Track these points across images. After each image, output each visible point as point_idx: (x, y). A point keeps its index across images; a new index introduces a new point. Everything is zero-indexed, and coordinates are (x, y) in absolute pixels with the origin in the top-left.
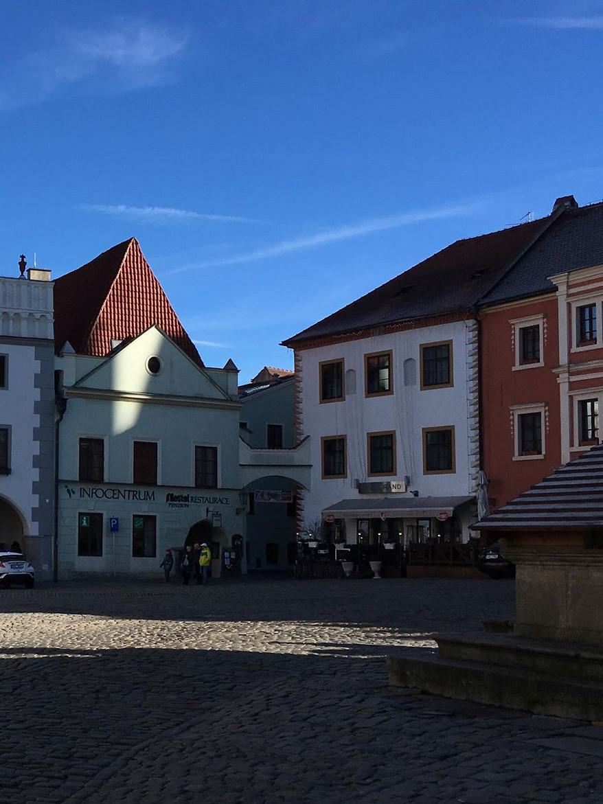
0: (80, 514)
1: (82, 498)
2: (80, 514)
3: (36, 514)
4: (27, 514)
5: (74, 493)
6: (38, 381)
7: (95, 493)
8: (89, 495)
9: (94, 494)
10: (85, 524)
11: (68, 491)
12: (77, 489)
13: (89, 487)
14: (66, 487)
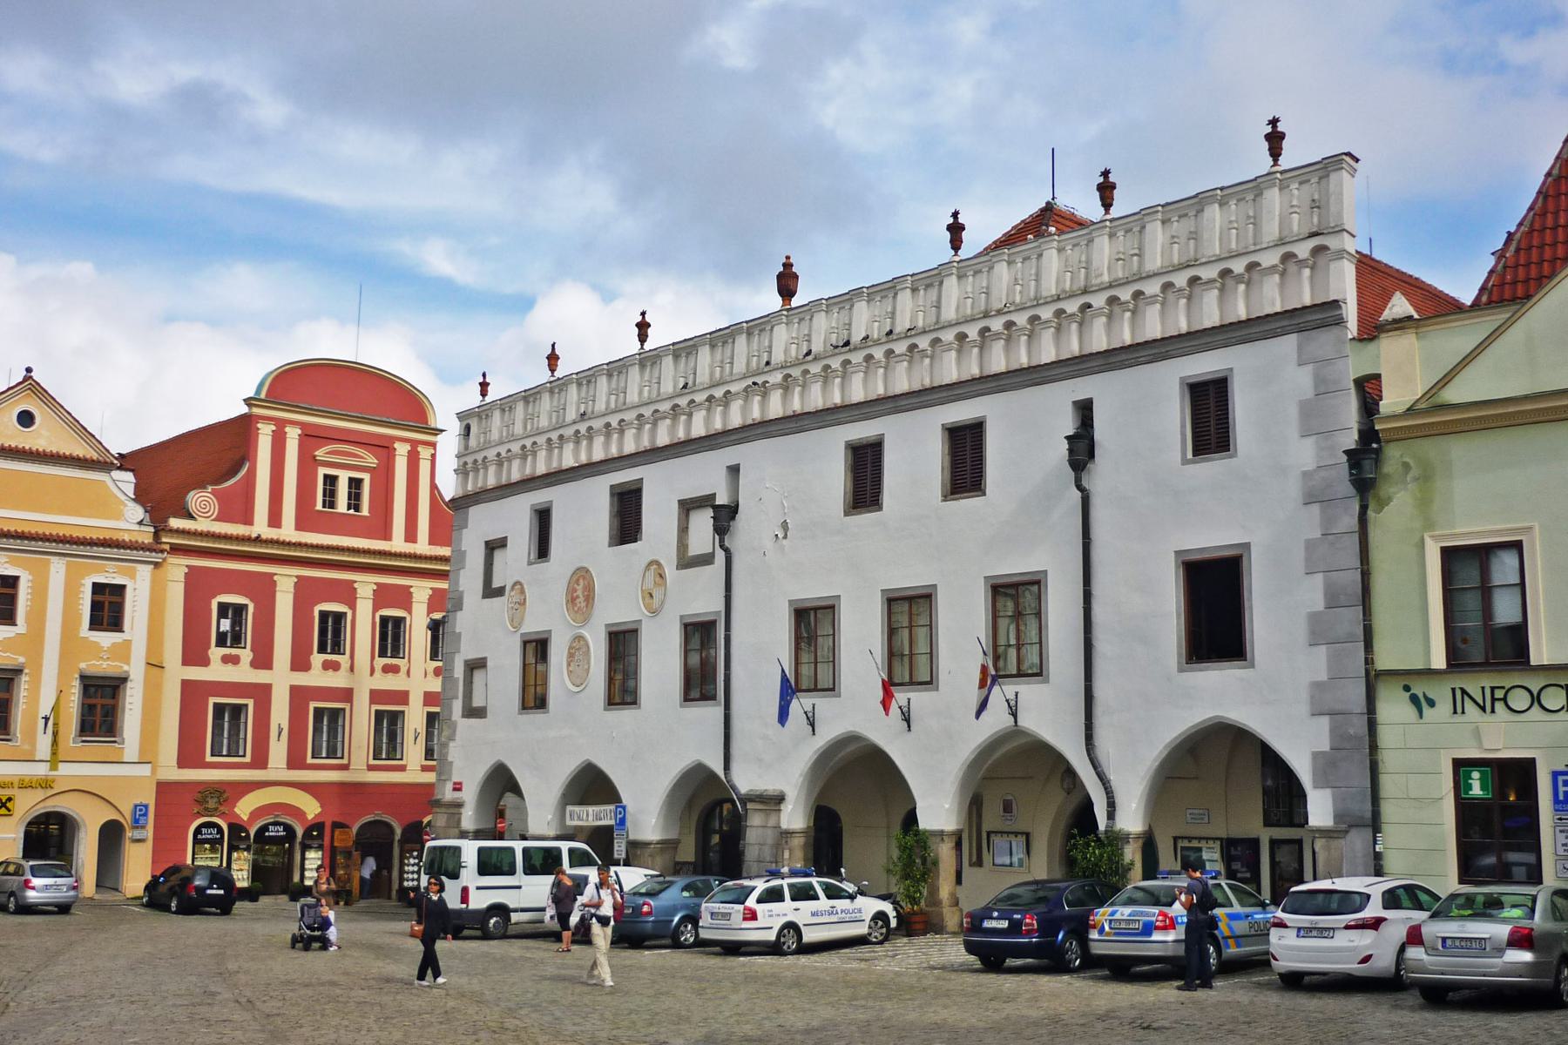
0: (1459, 764)
1: (1459, 718)
2: (1459, 764)
3: (1326, 767)
4: (1303, 769)
5: (1431, 703)
6: (1312, 420)
7: (1505, 699)
8: (1483, 709)
9: (1499, 706)
10: (1476, 790)
11: (1414, 699)
12: (1441, 693)
13: (1476, 684)
14: (1407, 688)
